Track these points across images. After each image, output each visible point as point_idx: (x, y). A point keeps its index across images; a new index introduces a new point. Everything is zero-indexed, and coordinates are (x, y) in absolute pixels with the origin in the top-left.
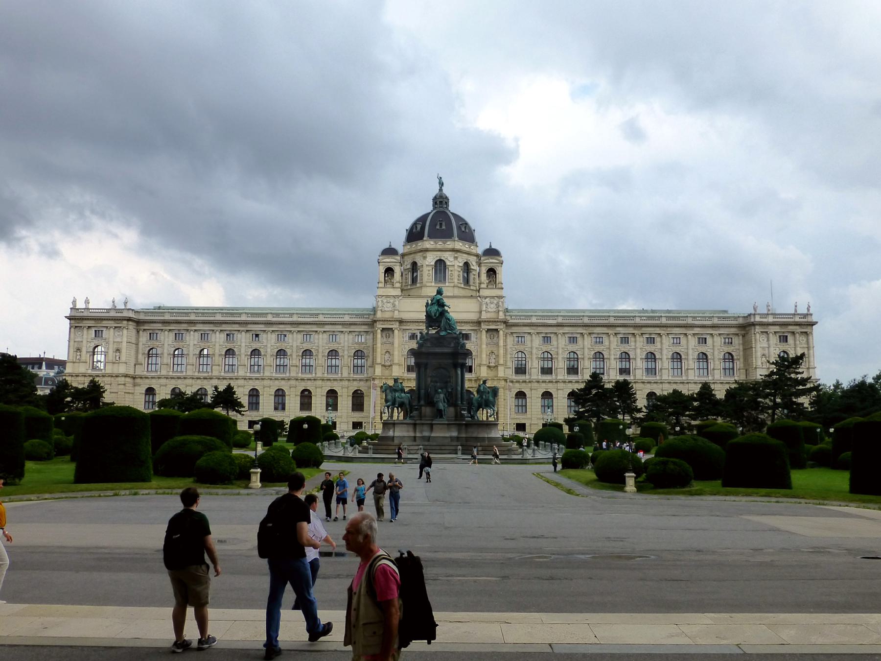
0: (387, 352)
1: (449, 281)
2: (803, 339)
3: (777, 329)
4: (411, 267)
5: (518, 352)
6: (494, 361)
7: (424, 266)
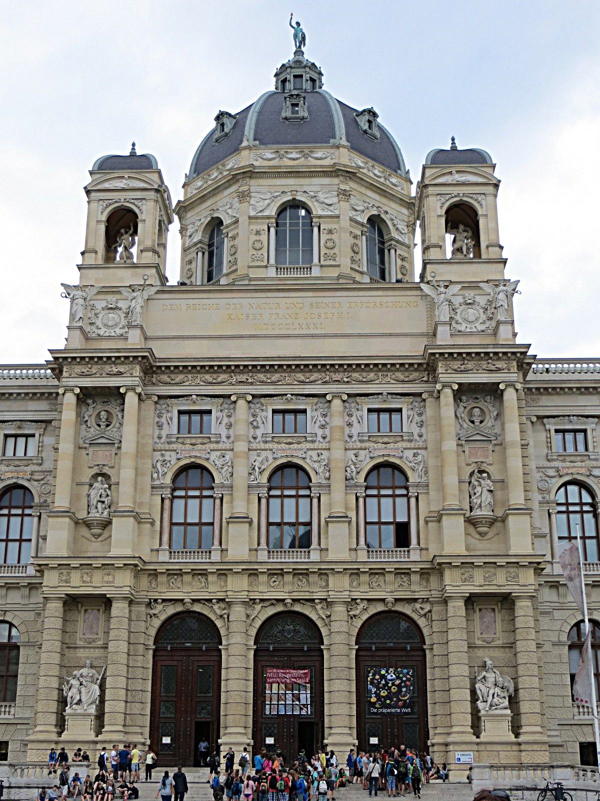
0: (97, 475)
1: (322, 263)
4: (206, 240)
5: (565, 484)
6: (487, 498)
7: (243, 220)
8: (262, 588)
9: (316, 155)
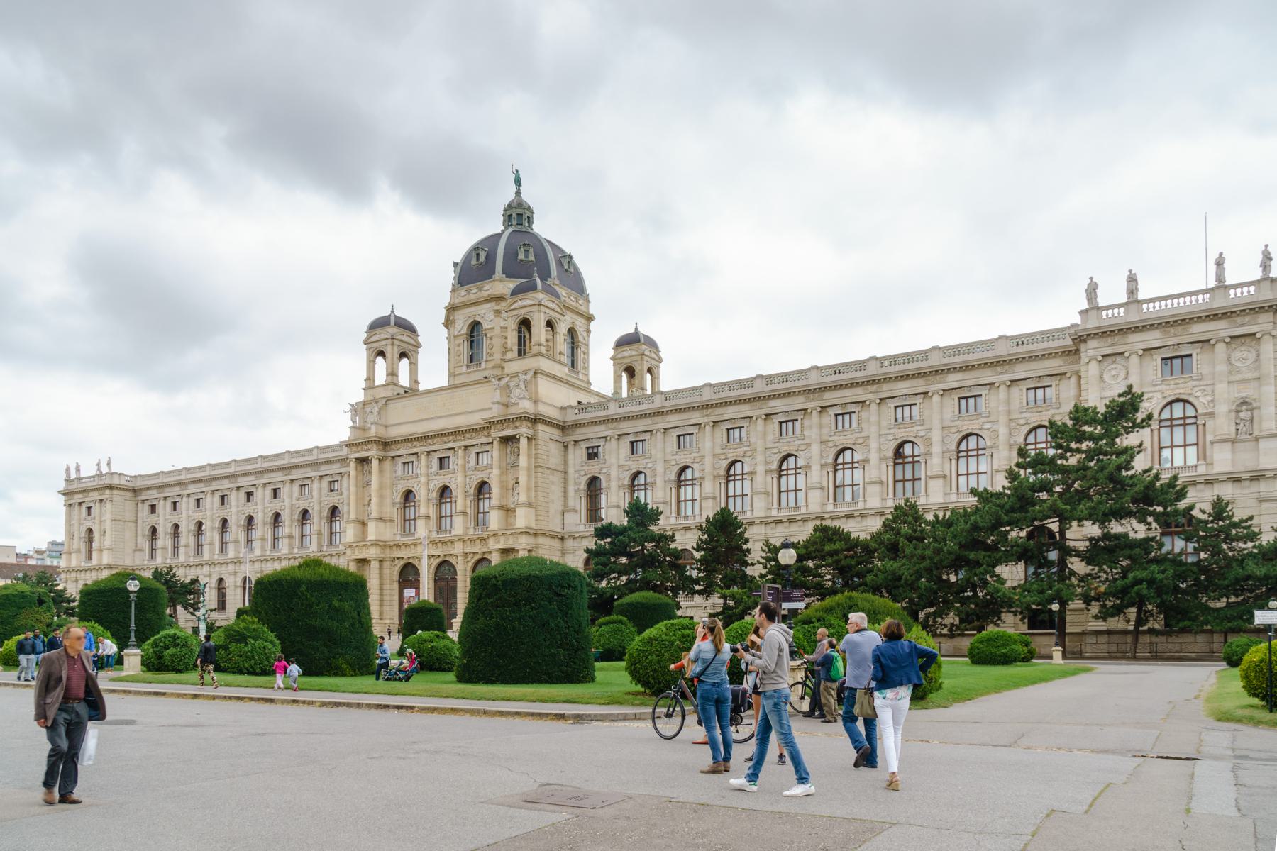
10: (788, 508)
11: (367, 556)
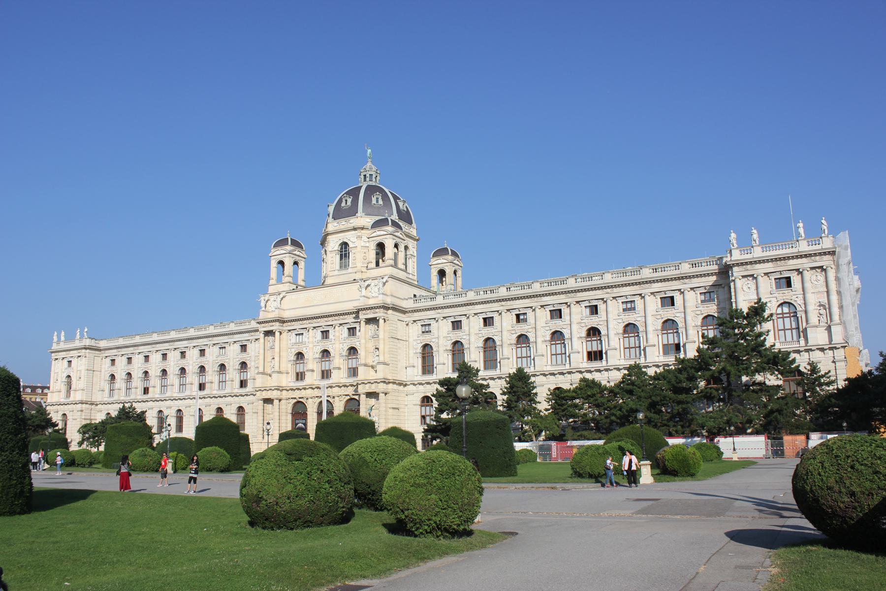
2: (819, 277)
3: (769, 267)
8: (316, 393)
9: (350, 222)
10: (557, 364)
11: (272, 397)
